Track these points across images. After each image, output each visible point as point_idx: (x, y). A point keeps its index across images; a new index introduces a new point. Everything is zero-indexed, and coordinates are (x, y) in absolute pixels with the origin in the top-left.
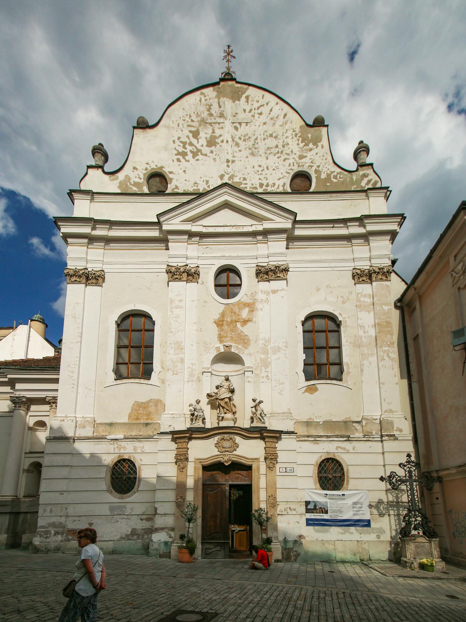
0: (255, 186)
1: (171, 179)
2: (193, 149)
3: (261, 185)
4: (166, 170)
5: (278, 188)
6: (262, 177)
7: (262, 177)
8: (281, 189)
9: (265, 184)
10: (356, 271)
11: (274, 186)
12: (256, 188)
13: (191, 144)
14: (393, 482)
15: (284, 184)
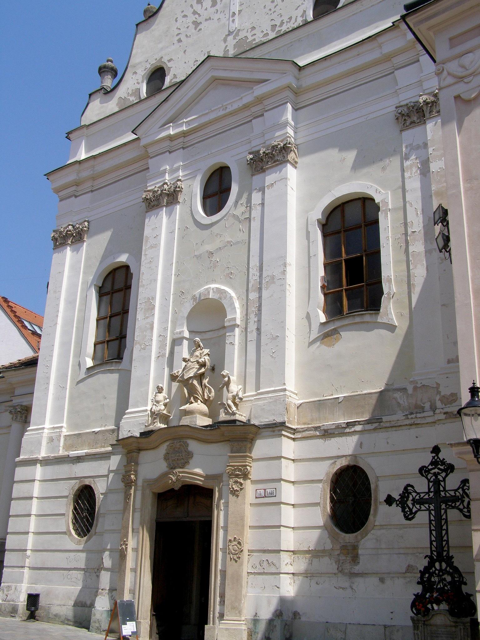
0: (265, 32)
1: (170, 68)
2: (196, 18)
3: (274, 27)
4: (165, 60)
5: (296, 21)
6: (274, 16)
7: (274, 16)
8: (300, 21)
9: (278, 25)
10: (399, 111)
11: (289, 22)
12: (267, 34)
13: (195, 13)
14: (408, 506)
15: (305, 11)
